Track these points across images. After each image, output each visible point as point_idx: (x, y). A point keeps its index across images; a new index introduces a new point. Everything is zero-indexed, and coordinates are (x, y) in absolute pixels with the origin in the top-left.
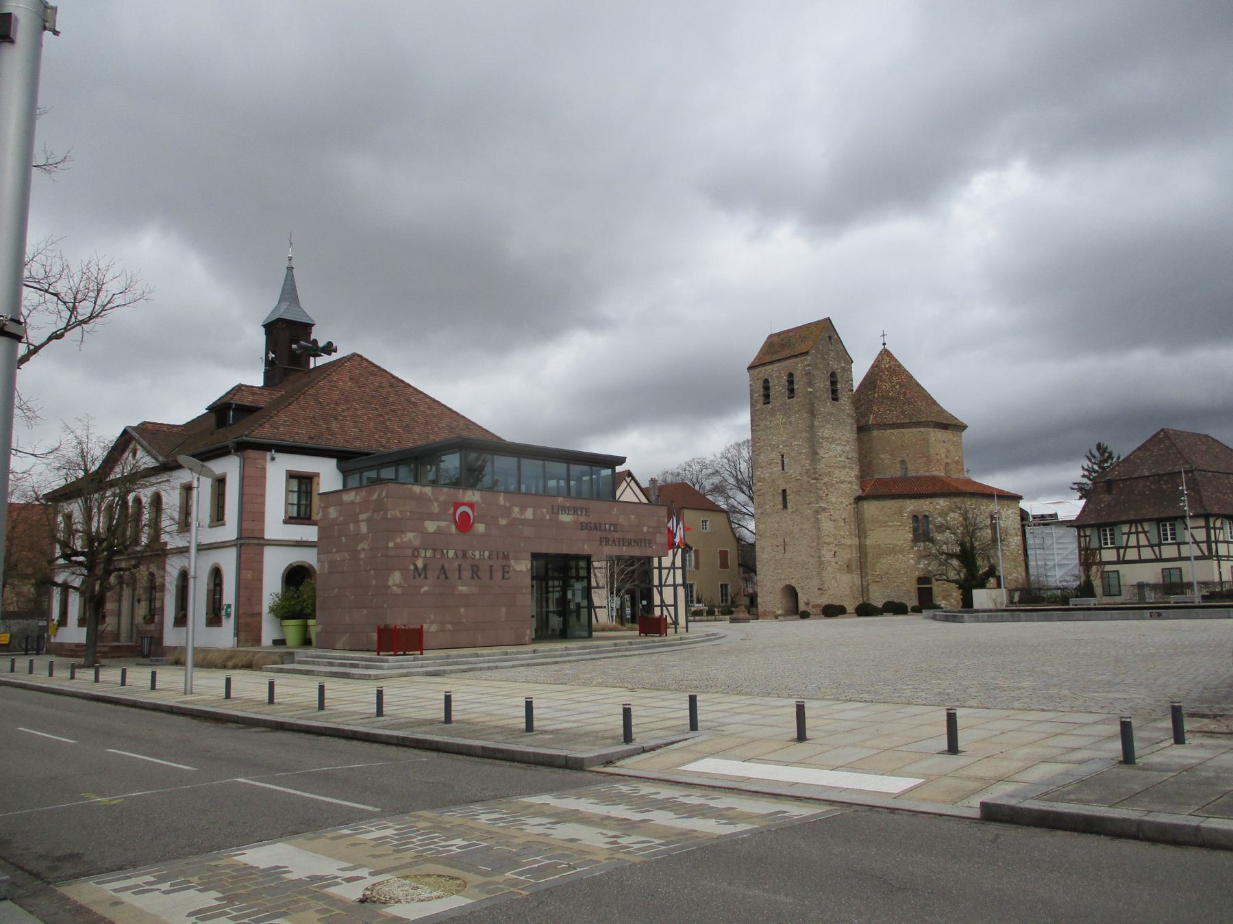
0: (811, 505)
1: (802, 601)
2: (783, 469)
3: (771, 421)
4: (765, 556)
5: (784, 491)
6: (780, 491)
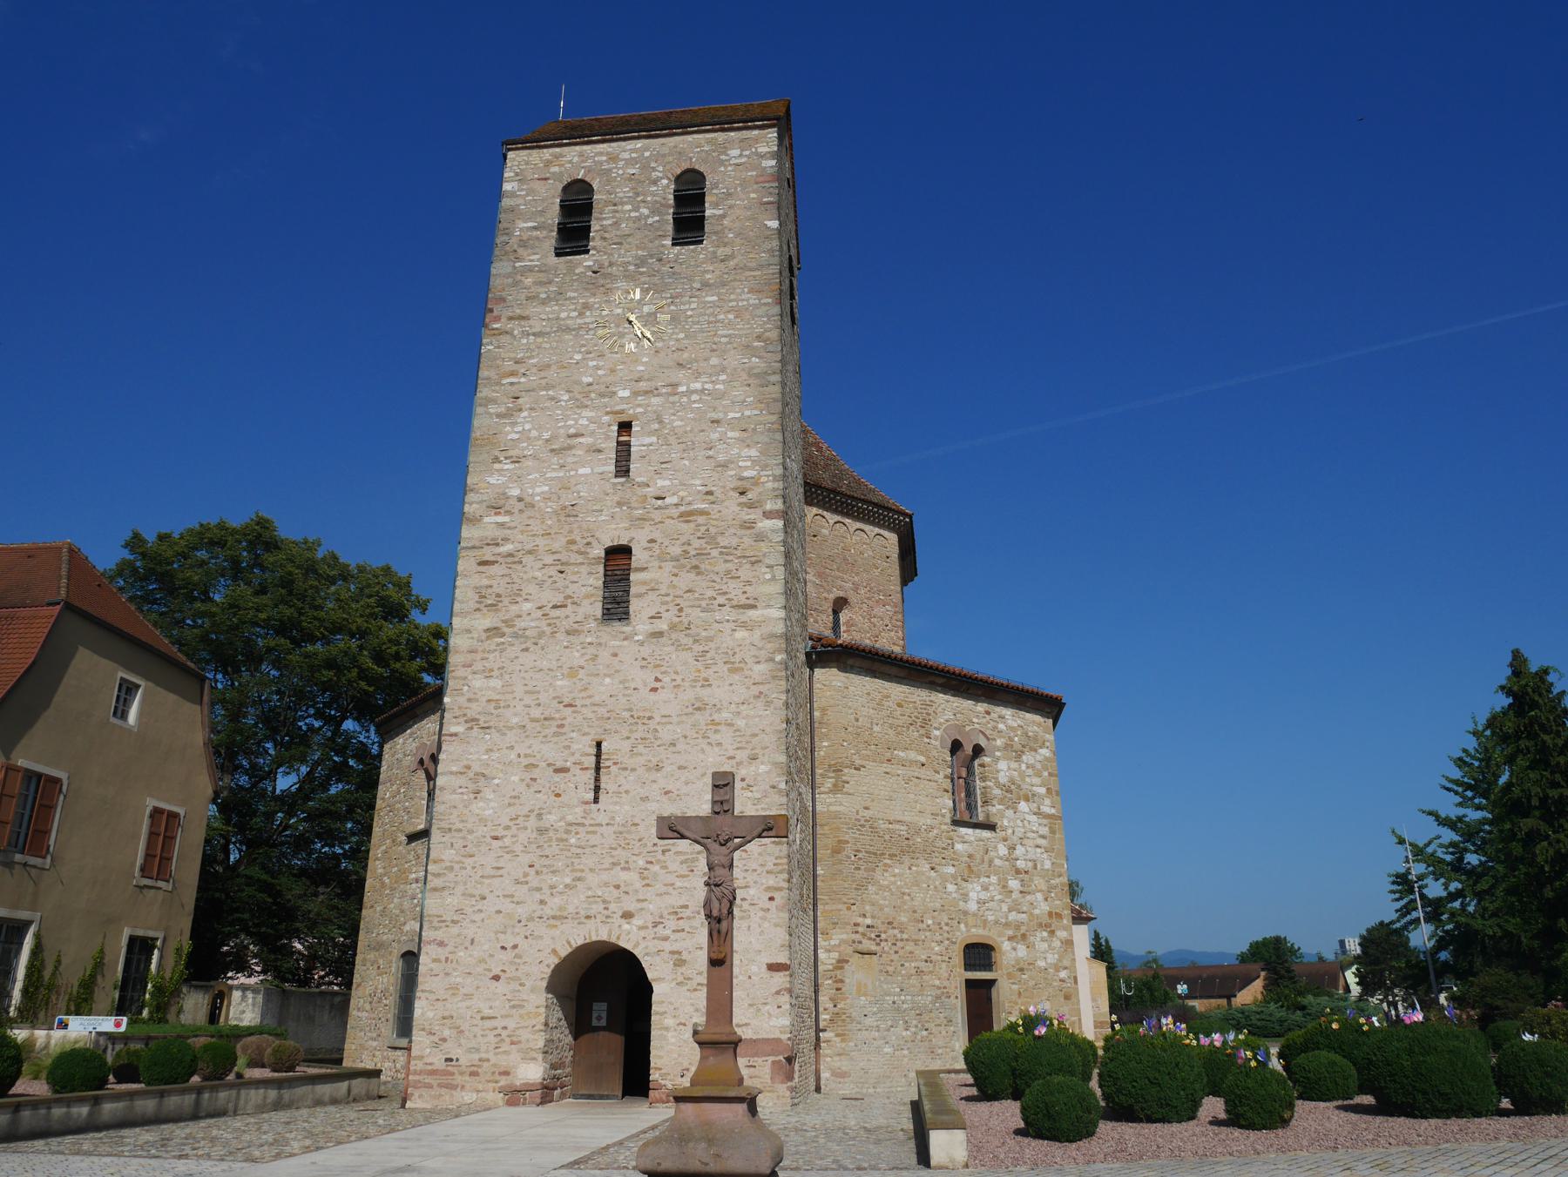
0: (751, 613)
1: (669, 1022)
2: (623, 469)
3: (586, 306)
4: (489, 806)
5: (618, 555)
6: (599, 552)
